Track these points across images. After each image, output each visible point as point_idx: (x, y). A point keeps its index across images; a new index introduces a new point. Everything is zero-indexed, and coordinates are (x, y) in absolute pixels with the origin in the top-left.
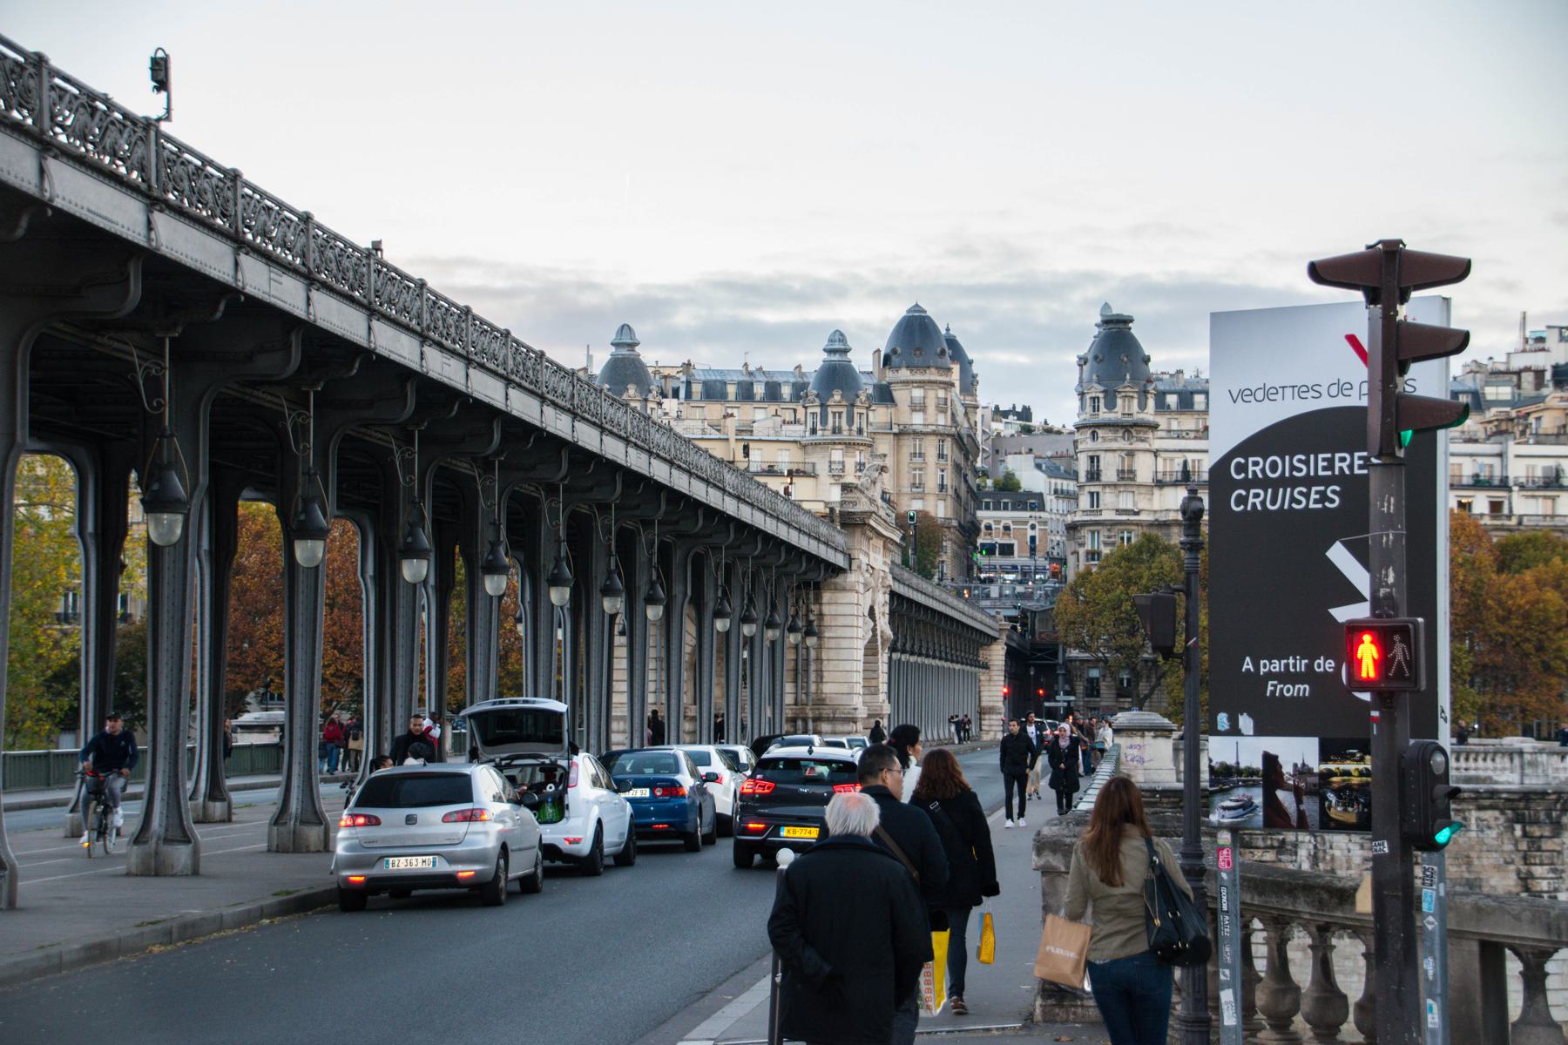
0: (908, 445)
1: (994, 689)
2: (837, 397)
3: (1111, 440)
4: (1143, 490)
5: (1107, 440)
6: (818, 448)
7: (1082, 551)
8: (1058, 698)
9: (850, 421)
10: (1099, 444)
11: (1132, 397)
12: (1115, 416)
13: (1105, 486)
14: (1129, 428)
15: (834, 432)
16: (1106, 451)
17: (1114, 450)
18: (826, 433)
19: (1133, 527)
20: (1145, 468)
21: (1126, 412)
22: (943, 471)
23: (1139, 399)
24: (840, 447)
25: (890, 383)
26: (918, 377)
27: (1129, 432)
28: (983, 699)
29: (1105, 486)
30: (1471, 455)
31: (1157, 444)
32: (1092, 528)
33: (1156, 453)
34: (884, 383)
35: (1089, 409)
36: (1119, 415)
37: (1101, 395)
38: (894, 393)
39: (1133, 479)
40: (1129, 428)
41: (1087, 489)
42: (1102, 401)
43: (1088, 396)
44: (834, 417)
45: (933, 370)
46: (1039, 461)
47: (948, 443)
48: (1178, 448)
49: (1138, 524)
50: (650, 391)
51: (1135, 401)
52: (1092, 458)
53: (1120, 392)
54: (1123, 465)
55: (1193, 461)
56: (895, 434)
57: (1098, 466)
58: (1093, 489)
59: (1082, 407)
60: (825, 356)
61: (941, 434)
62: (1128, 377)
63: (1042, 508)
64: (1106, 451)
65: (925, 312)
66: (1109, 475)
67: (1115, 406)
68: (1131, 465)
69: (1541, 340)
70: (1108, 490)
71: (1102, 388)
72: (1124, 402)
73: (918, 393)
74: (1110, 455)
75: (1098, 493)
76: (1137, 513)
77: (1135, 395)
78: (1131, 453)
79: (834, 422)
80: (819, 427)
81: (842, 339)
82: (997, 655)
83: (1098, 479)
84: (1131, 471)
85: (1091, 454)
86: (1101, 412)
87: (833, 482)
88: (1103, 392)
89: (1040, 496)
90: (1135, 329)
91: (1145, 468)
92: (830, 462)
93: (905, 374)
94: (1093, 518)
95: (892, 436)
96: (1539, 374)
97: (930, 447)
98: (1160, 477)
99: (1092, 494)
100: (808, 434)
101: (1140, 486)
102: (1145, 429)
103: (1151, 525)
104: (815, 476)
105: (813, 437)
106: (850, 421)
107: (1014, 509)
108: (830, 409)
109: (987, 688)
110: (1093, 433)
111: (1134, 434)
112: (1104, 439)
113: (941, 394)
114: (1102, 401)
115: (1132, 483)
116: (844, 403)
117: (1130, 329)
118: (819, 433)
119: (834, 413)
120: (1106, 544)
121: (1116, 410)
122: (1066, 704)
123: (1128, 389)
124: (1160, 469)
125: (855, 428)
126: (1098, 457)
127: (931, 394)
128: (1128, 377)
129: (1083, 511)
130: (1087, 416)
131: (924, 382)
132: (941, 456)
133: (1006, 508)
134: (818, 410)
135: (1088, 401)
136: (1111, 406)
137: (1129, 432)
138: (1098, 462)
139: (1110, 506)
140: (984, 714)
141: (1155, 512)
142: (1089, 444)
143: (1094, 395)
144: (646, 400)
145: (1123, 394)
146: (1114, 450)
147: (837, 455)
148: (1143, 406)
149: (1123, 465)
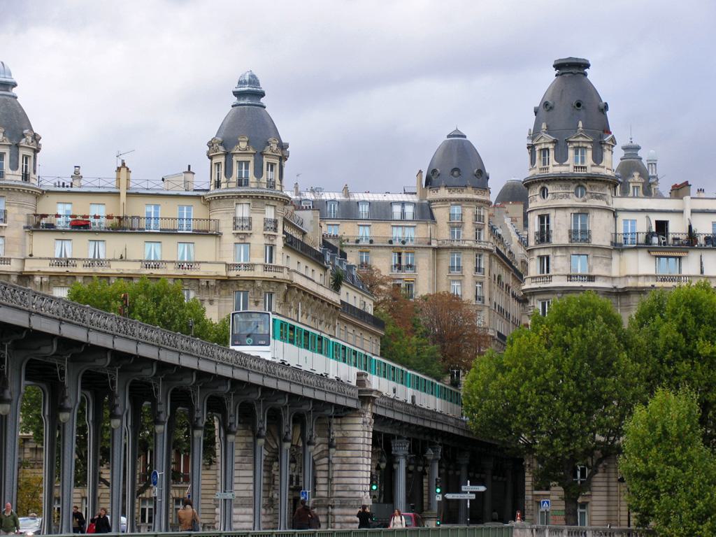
0: (446, 259)
2: (243, 145)
3: (562, 197)
4: (599, 253)
6: (222, 204)
8: (463, 488)
9: (258, 173)
10: (549, 202)
11: (586, 148)
12: (568, 169)
13: (556, 248)
14: (581, 182)
15: (240, 184)
16: (557, 208)
17: (565, 208)
18: (231, 185)
20: (601, 229)
21: (580, 164)
23: (593, 149)
25: (430, 202)
26: (456, 195)
29: (556, 248)
31: (619, 203)
32: (541, 297)
33: (615, 213)
35: (538, 163)
37: (551, 146)
38: (434, 211)
39: (587, 240)
40: (581, 182)
41: (537, 253)
42: (552, 153)
43: (537, 148)
44: (240, 168)
47: (485, 260)
48: (639, 208)
50: (23, 136)
51: (589, 154)
52: (542, 218)
54: (576, 225)
56: (434, 249)
57: (548, 226)
58: (543, 253)
59: (533, 162)
60: (235, 100)
61: (477, 249)
62: (580, 124)
64: (557, 208)
65: (465, 137)
66: (560, 235)
67: (566, 159)
68: (583, 226)
70: (558, 253)
72: (577, 153)
73: (456, 210)
74: (560, 214)
75: (548, 258)
76: (591, 278)
77: (589, 146)
78: (584, 212)
79: (240, 173)
80: (223, 179)
81: (254, 81)
82: (360, 432)
83: (548, 240)
85: (540, 213)
88: (554, 142)
90: (591, 74)
91: (601, 229)
92: (235, 218)
93: (443, 193)
95: (431, 251)
98: (620, 240)
99: (541, 258)
102: (601, 185)
103: (609, 293)
104: (218, 235)
105: (217, 191)
106: (258, 173)
108: (235, 159)
111: (588, 190)
116: (251, 151)
117: (585, 74)
118: (223, 186)
119: (240, 163)
121: (567, 163)
122: (473, 497)
123: (581, 139)
124: (621, 230)
125: (264, 179)
126: (548, 216)
128: (580, 124)
129: (532, 278)
131: (461, 200)
132: (478, 269)
134: (222, 159)
136: (561, 159)
138: (548, 222)
139: (561, 272)
141: (613, 278)
143: (543, 146)
144: (18, 146)
145: (575, 145)
146: (565, 208)
147: (243, 211)
148: (598, 159)
149: (576, 225)
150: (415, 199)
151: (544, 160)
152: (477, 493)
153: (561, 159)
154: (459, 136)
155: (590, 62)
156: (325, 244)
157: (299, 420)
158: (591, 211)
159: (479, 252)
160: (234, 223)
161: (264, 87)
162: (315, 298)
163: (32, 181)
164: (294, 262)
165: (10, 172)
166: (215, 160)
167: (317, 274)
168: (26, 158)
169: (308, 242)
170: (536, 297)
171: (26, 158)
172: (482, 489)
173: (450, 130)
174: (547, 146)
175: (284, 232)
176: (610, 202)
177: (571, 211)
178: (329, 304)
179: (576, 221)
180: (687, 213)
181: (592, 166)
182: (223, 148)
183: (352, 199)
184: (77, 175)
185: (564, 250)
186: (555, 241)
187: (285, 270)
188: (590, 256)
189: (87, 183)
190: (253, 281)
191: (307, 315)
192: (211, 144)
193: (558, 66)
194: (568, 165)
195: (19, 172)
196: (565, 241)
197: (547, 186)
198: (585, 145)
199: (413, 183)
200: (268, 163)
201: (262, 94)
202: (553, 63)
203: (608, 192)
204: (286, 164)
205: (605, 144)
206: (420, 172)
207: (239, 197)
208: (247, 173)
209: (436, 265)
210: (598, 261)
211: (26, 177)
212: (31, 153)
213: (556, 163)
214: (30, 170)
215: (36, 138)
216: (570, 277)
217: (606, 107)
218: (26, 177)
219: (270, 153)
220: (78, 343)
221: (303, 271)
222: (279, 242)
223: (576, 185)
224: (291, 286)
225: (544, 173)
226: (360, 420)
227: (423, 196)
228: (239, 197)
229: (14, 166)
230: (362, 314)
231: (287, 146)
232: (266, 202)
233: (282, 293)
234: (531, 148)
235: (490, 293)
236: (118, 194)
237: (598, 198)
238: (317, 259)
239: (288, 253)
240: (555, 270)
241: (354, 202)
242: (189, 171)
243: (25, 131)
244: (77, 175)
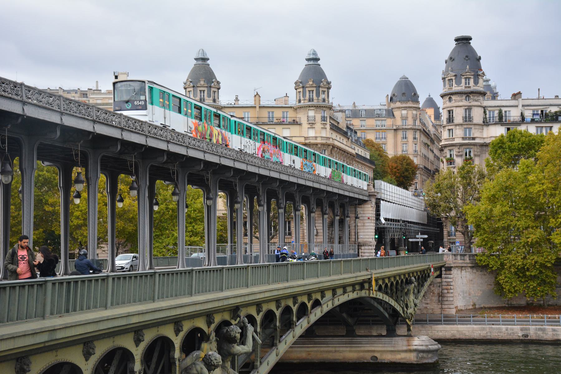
0: (400, 134)
1: (366, 231)
2: (311, 83)
3: (459, 101)
4: (477, 127)
5: (457, 101)
6: (302, 110)
9: (318, 95)
10: (453, 103)
12: (462, 88)
13: (456, 125)
14: (468, 94)
19: (472, 147)
20: (477, 115)
21: (467, 85)
22: (416, 144)
23: (474, 78)
24: (312, 108)
25: (392, 109)
26: (404, 105)
27: (468, 96)
28: (360, 237)
29: (456, 125)
34: (390, 108)
35: (447, 86)
36: (463, 88)
37: (453, 78)
40: (468, 94)
41: (447, 128)
42: (454, 81)
43: (447, 79)
44: (310, 93)
45: (410, 102)
47: (418, 135)
49: (475, 145)
50: (213, 82)
51: (472, 81)
52: (449, 111)
53: (463, 75)
54: (466, 114)
55: (506, 112)
56: (395, 130)
57: (452, 115)
58: (450, 127)
59: (445, 85)
60: (307, 63)
61: (415, 129)
62: (468, 67)
67: (461, 83)
70: (458, 127)
71: (454, 74)
72: (466, 80)
73: (404, 112)
74: (458, 109)
76: (474, 139)
77: (472, 77)
78: (469, 109)
79: (310, 96)
80: (302, 98)
81: (315, 53)
85: (449, 109)
86: (453, 87)
87: (309, 126)
88: (455, 76)
92: (308, 116)
93: (398, 104)
94: (450, 142)
95: (393, 131)
97: (410, 135)
99: (449, 130)
100: (297, 103)
101: (475, 125)
102: (478, 95)
105: (299, 104)
106: (318, 95)
109: (362, 231)
110: (450, 98)
111: (472, 97)
112: (455, 101)
113: (415, 112)
114: (454, 81)
115: (471, 123)
116: (314, 85)
117: (470, 43)
118: (302, 102)
119: (309, 91)
120: (457, 156)
121: (461, 85)
122: (422, 240)
123: (468, 74)
125: (320, 98)
126: (452, 110)
127: (410, 112)
129: (445, 139)
130: (447, 90)
131: (406, 107)
132: (415, 138)
135: (447, 82)
136: (459, 83)
137: (468, 96)
138: (452, 113)
140: (361, 246)
141: (484, 138)
142: (448, 104)
143: (450, 78)
146: (461, 106)
147: (311, 113)
148: (476, 83)
150: (386, 107)
151: (450, 84)
152: (424, 239)
153: (459, 83)
154: (405, 78)
155: (472, 37)
156: (348, 128)
157: (342, 206)
158: (473, 107)
159: (415, 130)
160: (308, 119)
161: (319, 56)
162: (344, 152)
163: (217, 102)
164: (334, 135)
165: (208, 99)
166: (298, 90)
167: (345, 141)
168: (214, 92)
169: (340, 126)
170: (448, 148)
171: (214, 92)
172: (426, 236)
173: (401, 76)
174: (452, 78)
175: (330, 122)
176: (482, 102)
177: (464, 108)
178: (351, 155)
179: (466, 112)
180: (520, 107)
181: (474, 86)
182: (301, 85)
183: (357, 108)
184: (237, 100)
185: (460, 126)
187: (331, 139)
188: (473, 128)
189: (241, 103)
190: (317, 144)
191: (341, 159)
192: (296, 83)
193: (457, 40)
194: (462, 86)
195: (211, 98)
197: (451, 96)
198: (470, 76)
199: (384, 101)
200: (322, 91)
201: (319, 59)
202: (454, 39)
203: (481, 98)
204: (330, 91)
205: (479, 75)
206: (388, 95)
207: (310, 106)
208: (313, 96)
209: (395, 136)
210: (477, 130)
211: (214, 101)
212: (216, 90)
213: (456, 86)
214: (216, 98)
215: (218, 83)
216: (463, 138)
217: (480, 58)
218: (214, 101)
219: (323, 86)
220: (243, 171)
221: (338, 139)
222: (328, 127)
223: (466, 95)
224: (334, 147)
225: (451, 91)
226: (370, 206)
227: (389, 105)
228: (310, 106)
229: (209, 96)
230: (364, 159)
231: (331, 83)
232: (322, 108)
233: (330, 149)
234: (444, 79)
235: (420, 149)
236: (255, 107)
237: (476, 101)
238: (345, 134)
239: (332, 132)
240: (456, 135)
241: (358, 110)
242: (286, 96)
243: (214, 80)
244: (237, 100)
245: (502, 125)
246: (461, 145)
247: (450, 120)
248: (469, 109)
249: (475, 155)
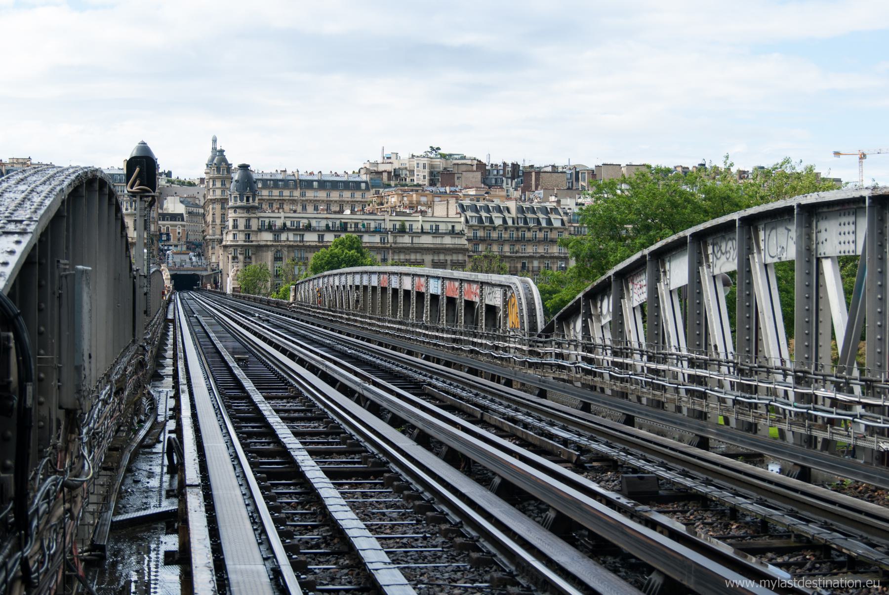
7: (230, 256)
12: (244, 203)
13: (239, 231)
20: (254, 224)
29: (239, 231)
30: (374, 220)
33: (258, 218)
40: (248, 209)
46: (182, 199)
52: (234, 220)
63: (183, 220)
69: (389, 158)
74: (241, 219)
76: (252, 242)
84: (249, 226)
89: (182, 214)
96: (389, 173)
101: (253, 231)
107: (171, 220)
120: (240, 254)
133: (167, 220)
148: (254, 200)
153: (242, 200)
173: (140, 141)
186: (239, 228)
196: (243, 229)
216: (245, 241)
225: (235, 205)
245: (271, 232)
246: (242, 246)
247: (235, 226)
248: (248, 220)
249: (252, 254)
